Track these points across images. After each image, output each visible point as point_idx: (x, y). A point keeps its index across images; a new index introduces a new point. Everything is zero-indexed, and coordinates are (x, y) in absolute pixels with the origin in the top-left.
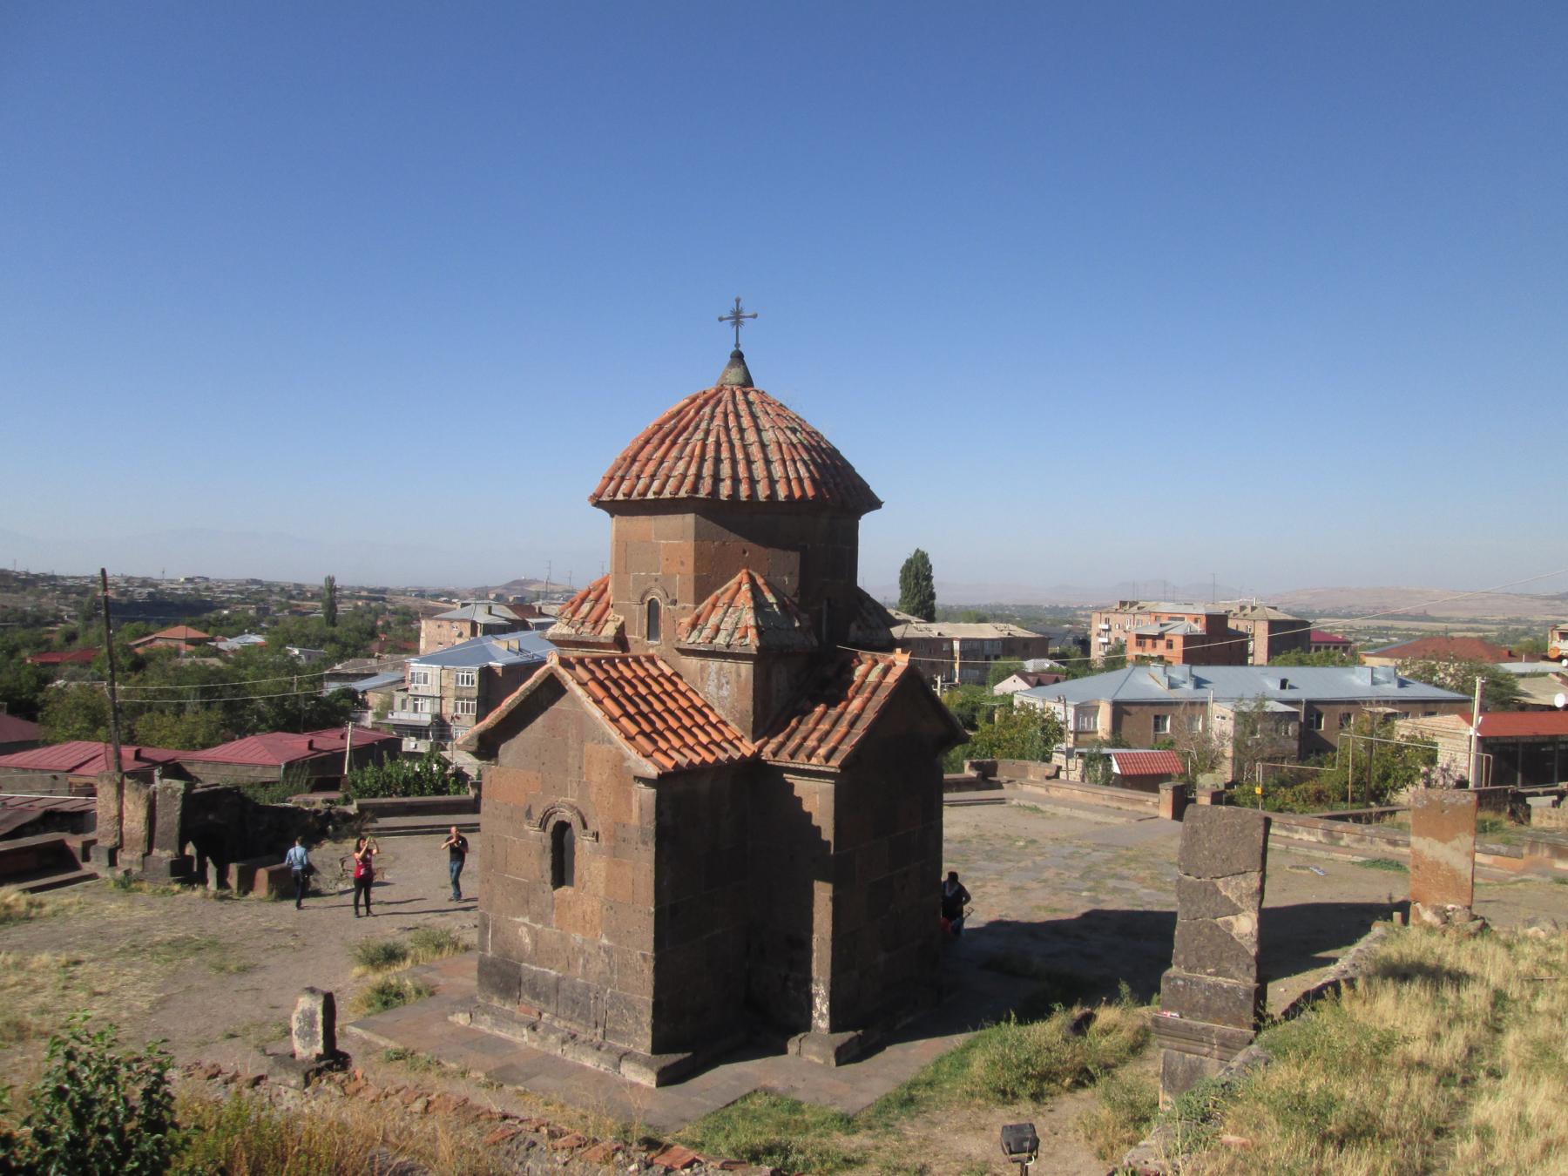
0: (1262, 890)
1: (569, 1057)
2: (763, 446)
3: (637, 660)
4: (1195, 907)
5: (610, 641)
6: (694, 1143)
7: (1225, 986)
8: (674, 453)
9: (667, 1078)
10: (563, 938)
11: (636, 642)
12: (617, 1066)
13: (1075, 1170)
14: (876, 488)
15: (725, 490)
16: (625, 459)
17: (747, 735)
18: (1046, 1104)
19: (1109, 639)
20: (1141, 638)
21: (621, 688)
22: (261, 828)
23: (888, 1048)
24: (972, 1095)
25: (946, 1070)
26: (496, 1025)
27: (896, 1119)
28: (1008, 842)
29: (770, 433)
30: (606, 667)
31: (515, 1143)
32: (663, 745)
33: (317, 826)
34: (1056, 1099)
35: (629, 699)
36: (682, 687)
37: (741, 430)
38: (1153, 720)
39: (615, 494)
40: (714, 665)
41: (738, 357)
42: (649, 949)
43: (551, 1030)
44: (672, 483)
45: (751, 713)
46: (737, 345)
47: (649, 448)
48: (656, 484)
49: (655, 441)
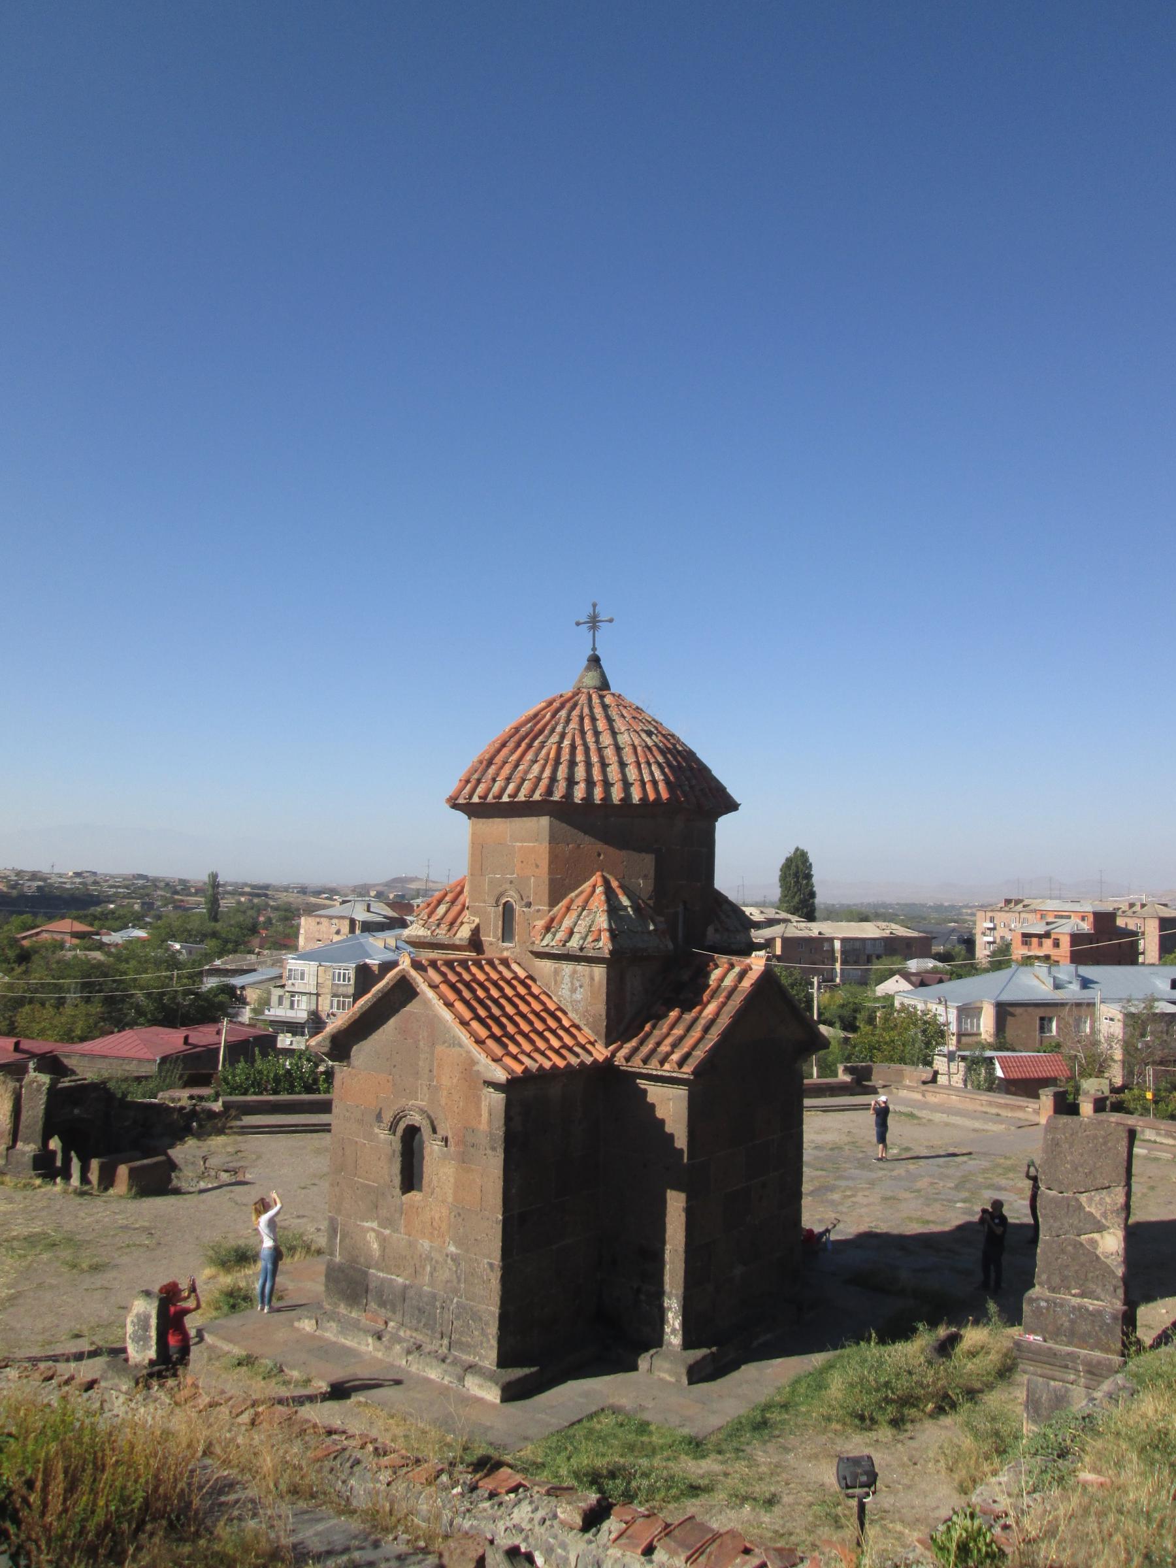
0: (1127, 1207)
1: (413, 1369)
2: (618, 749)
3: (491, 963)
4: (1057, 1224)
5: (465, 943)
6: (535, 1463)
7: (1091, 1308)
8: (529, 756)
9: (513, 1393)
10: (411, 1245)
11: (491, 944)
12: (461, 1379)
13: (934, 1505)
15: (579, 793)
16: (481, 762)
17: (600, 1039)
18: (906, 1431)
19: (994, 938)
20: (1027, 937)
21: (473, 991)
23: (743, 1367)
25: (802, 1391)
27: (748, 1444)
29: (626, 735)
30: (459, 969)
31: (338, 1461)
32: (513, 1049)
33: (182, 1123)
34: (918, 1425)
35: (481, 1002)
36: (536, 990)
37: (597, 734)
38: (1038, 1022)
39: (471, 797)
40: (567, 968)
41: (595, 661)
42: (497, 1261)
44: (527, 786)
45: (604, 1017)
46: (594, 649)
47: (505, 751)
48: (511, 787)
49: (511, 745)
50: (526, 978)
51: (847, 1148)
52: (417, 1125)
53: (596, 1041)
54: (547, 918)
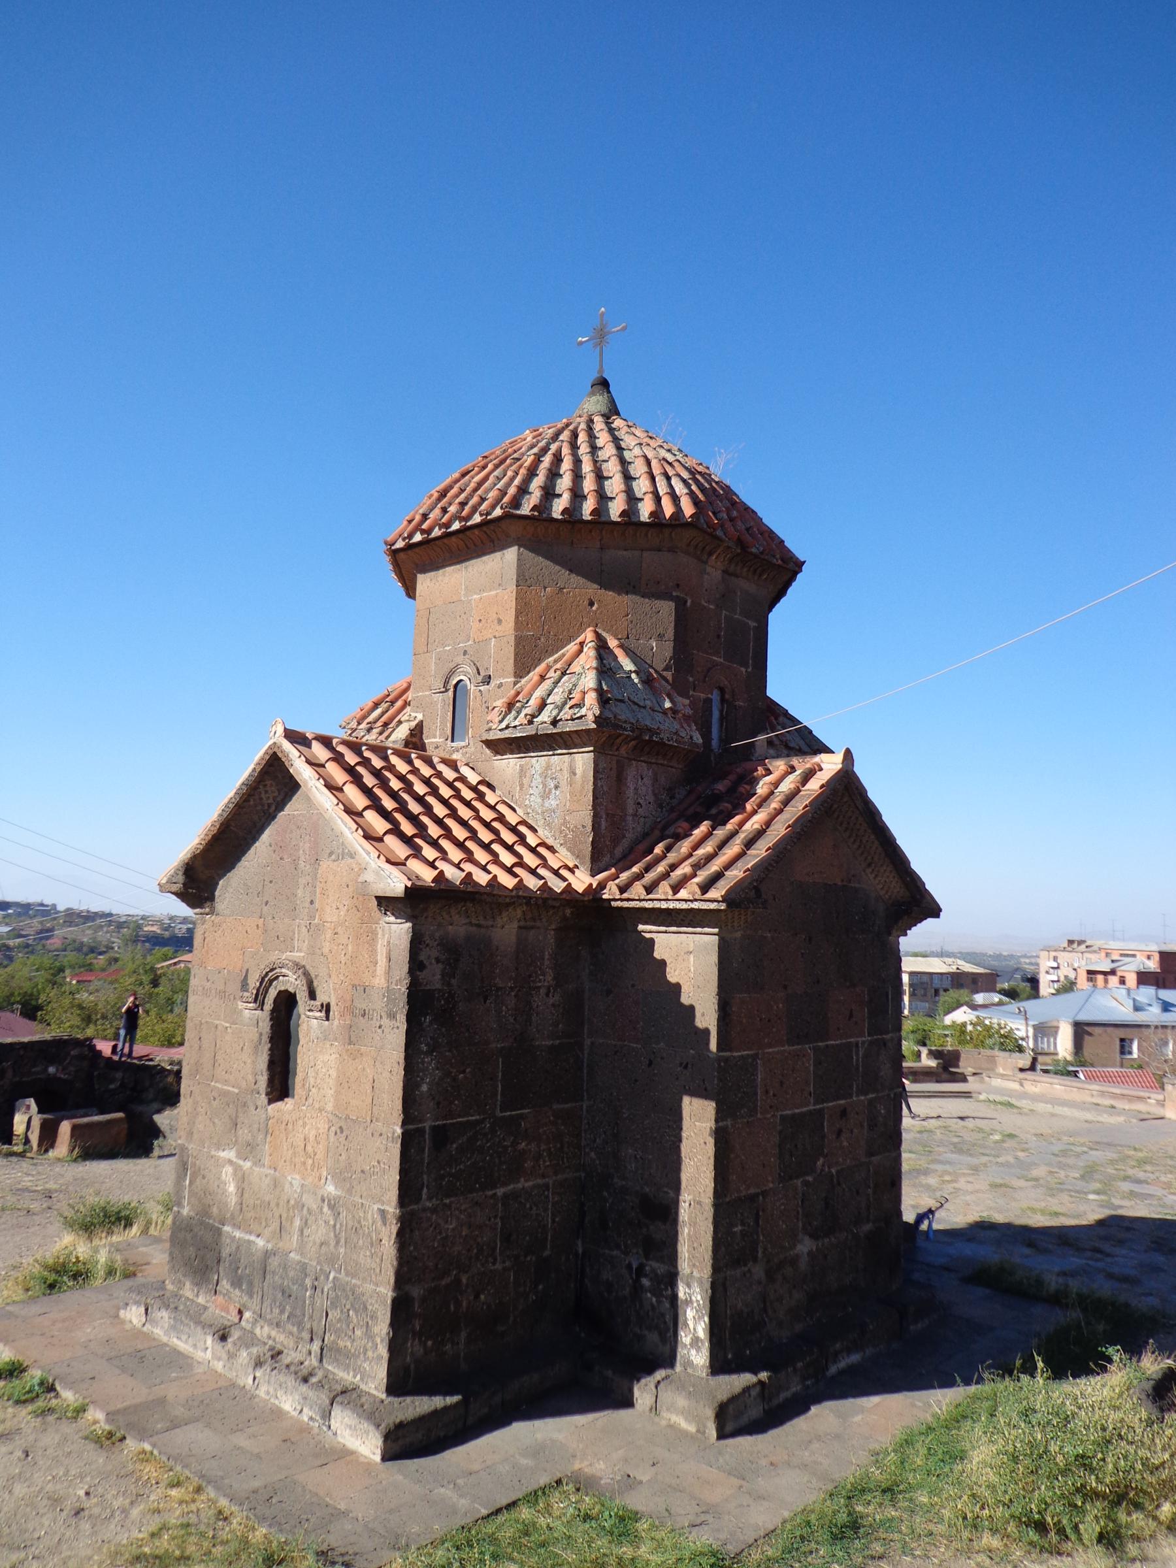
1: (262, 1392)
2: (624, 463)
10: (276, 1184)
12: (327, 1415)
14: (796, 545)
22: (112, 1086)
23: (814, 1409)
24: (975, 1527)
26: (173, 1327)
28: (981, 1135)
37: (594, 449)
38: (1118, 1042)
40: (537, 762)
42: (390, 1202)
43: (249, 1340)
45: (589, 828)
46: (601, 370)
50: (479, 783)
51: (938, 1131)
52: (291, 990)
53: (576, 867)
54: (512, 692)
